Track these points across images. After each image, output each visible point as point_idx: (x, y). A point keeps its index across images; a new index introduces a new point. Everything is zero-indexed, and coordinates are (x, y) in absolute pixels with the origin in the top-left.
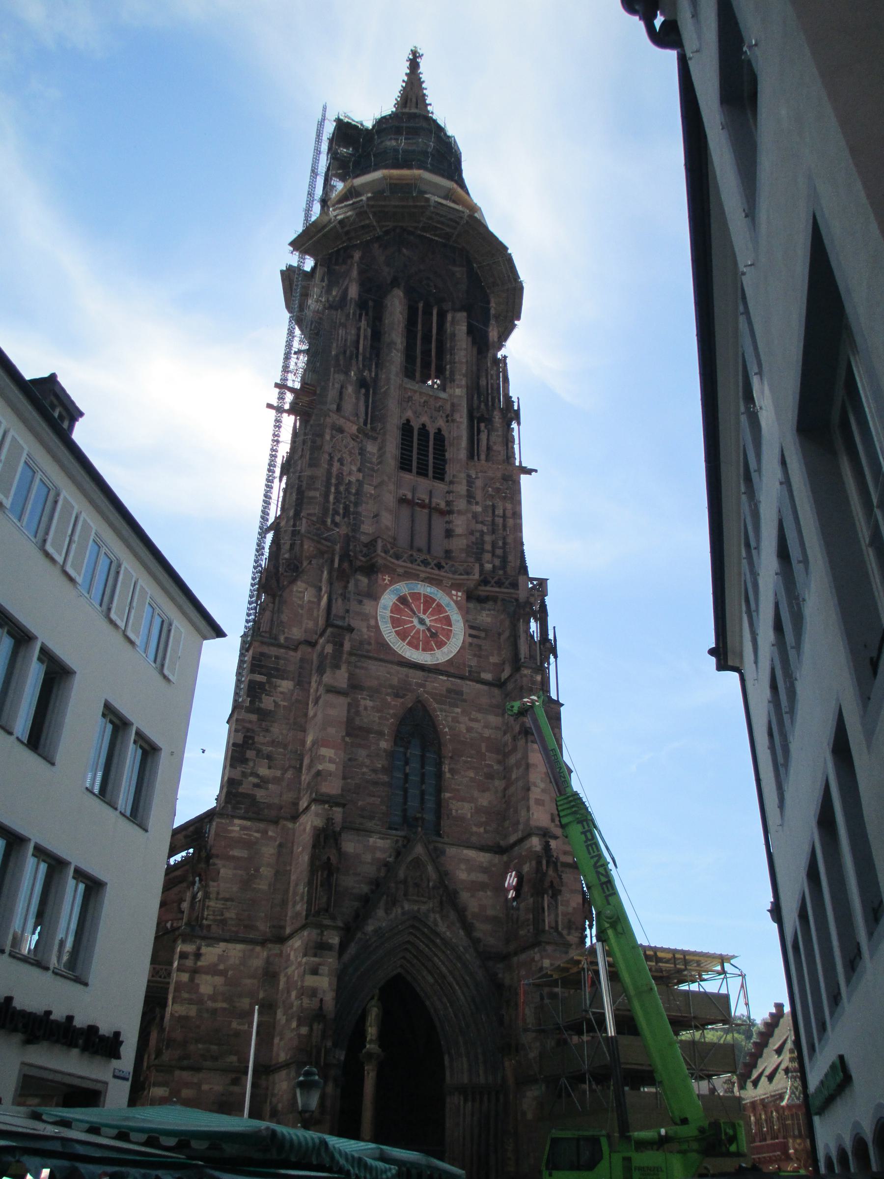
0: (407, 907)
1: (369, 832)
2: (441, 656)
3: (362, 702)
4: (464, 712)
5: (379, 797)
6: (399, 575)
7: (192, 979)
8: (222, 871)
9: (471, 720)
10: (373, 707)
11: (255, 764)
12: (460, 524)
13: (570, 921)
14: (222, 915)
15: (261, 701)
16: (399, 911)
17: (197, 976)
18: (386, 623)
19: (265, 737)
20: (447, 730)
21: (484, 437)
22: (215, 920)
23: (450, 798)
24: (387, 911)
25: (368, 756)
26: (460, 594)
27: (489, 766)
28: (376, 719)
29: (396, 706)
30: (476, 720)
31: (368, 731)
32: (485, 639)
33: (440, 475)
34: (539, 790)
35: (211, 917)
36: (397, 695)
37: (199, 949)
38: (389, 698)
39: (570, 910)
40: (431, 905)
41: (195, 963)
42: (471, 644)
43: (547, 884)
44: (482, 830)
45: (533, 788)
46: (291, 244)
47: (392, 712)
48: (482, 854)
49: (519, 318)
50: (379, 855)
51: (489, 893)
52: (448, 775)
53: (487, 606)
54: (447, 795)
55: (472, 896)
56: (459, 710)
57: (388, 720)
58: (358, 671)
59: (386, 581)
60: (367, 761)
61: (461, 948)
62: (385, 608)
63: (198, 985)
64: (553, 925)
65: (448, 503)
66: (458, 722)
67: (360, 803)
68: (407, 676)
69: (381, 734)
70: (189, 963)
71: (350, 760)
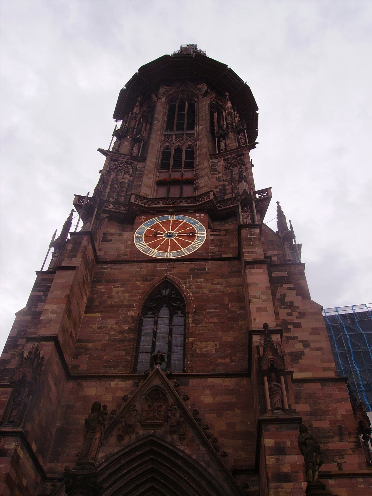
0: (141, 432)
1: (112, 378)
2: (185, 252)
3: (115, 290)
4: (206, 281)
5: (124, 350)
6: (152, 214)
9: (213, 284)
10: (124, 291)
11: (24, 347)
12: (202, 182)
13: (340, 428)
15: (36, 306)
16: (134, 436)
18: (142, 241)
19: (34, 328)
20: (191, 294)
21: (223, 144)
23: (194, 341)
24: (120, 438)
25: (116, 323)
26: (202, 215)
27: (232, 312)
28: (127, 298)
29: (144, 287)
30: (219, 284)
31: (120, 306)
32: (225, 235)
33: (190, 164)
34: (260, 301)
36: (146, 280)
38: (138, 283)
39: (339, 417)
40: (168, 427)
42: (212, 240)
43: (265, 367)
44: (228, 360)
45: (254, 300)
46: (114, 117)
47: (140, 291)
48: (228, 379)
49: (257, 109)
50: (120, 394)
51: (238, 411)
52: (192, 325)
53: (229, 220)
54: (191, 339)
56: (202, 280)
57: (137, 296)
58: (113, 271)
59: (143, 219)
60: (116, 327)
61: (203, 464)
62: (141, 233)
64: (279, 405)
65: (195, 176)
66: (202, 288)
67: (105, 357)
68: (156, 267)
69: (130, 307)
71: (99, 328)
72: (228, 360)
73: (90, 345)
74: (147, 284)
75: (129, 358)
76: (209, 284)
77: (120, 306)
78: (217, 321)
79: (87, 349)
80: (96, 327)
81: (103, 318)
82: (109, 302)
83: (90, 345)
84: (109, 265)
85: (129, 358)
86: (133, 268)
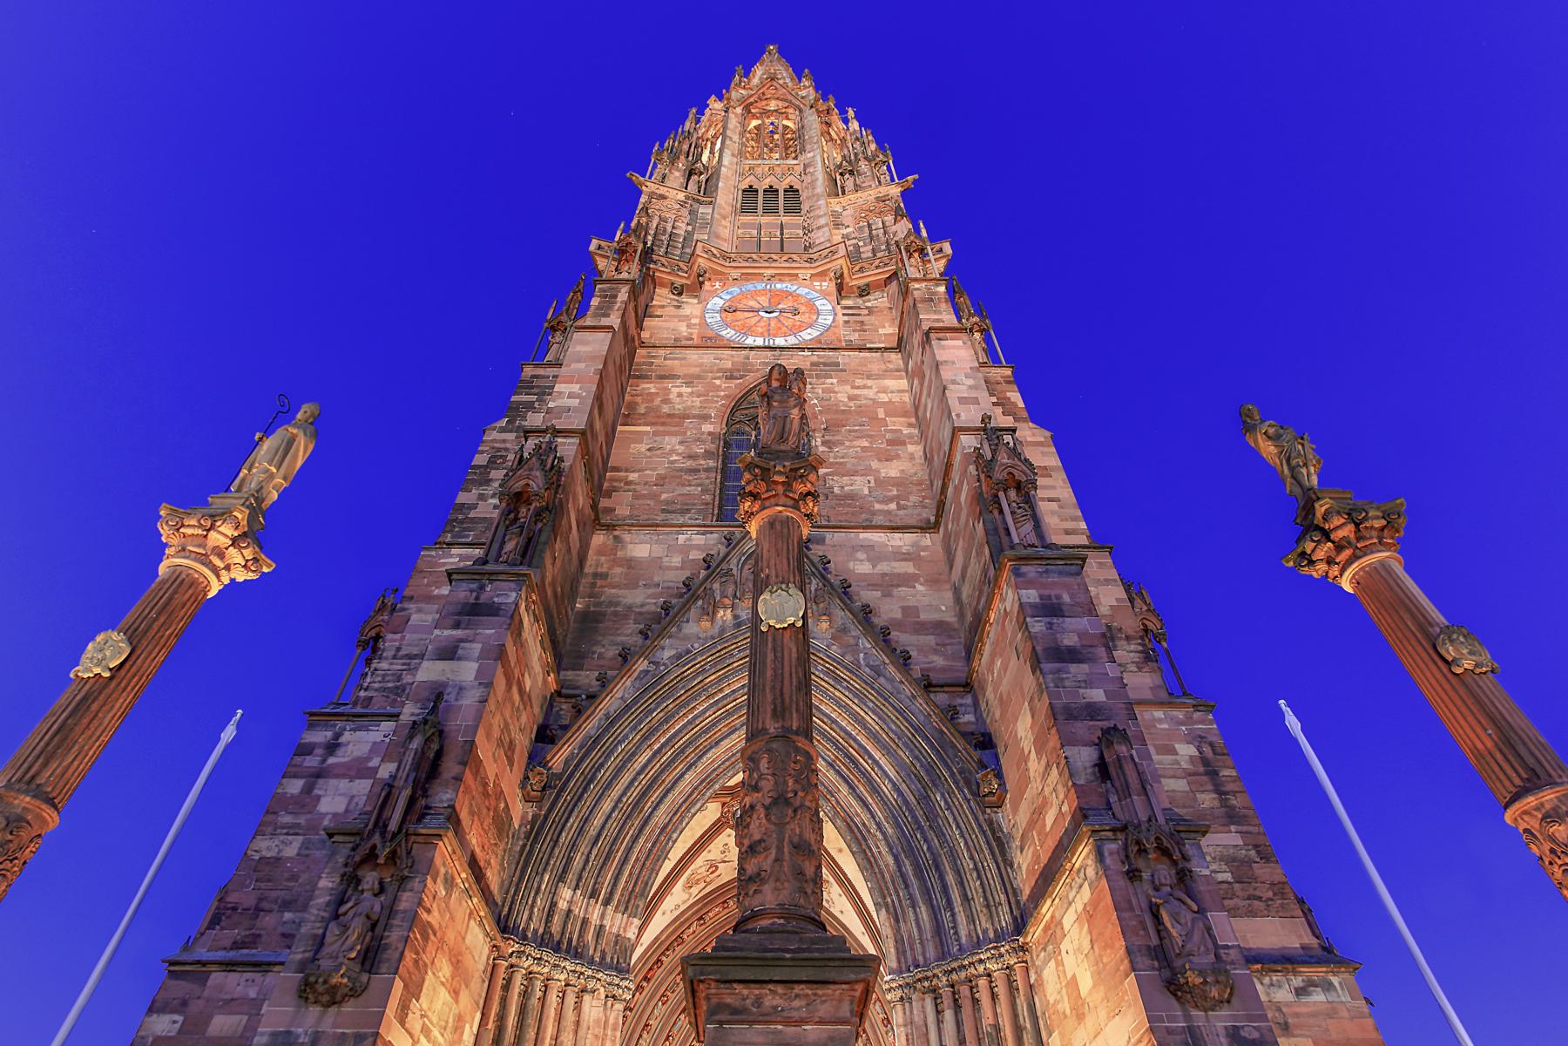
7: (308, 790)
8: (414, 617)
14: (399, 678)
17: (321, 781)
22: (385, 689)
30: (865, 387)
31: (685, 417)
35: (376, 685)
36: (732, 378)
37: (338, 736)
38: (718, 382)
41: (324, 761)
44: (893, 506)
50: (697, 555)
51: (919, 587)
55: (888, 595)
63: (318, 798)
67: (664, 496)
70: (311, 762)
72: (893, 506)
73: (633, 476)
74: (733, 384)
75: (708, 498)
76: (848, 388)
77: (685, 417)
78: (867, 444)
79: (628, 483)
80: (643, 448)
81: (655, 434)
82: (666, 409)
83: (633, 476)
84: (662, 352)
85: (708, 498)
86: (707, 357)
